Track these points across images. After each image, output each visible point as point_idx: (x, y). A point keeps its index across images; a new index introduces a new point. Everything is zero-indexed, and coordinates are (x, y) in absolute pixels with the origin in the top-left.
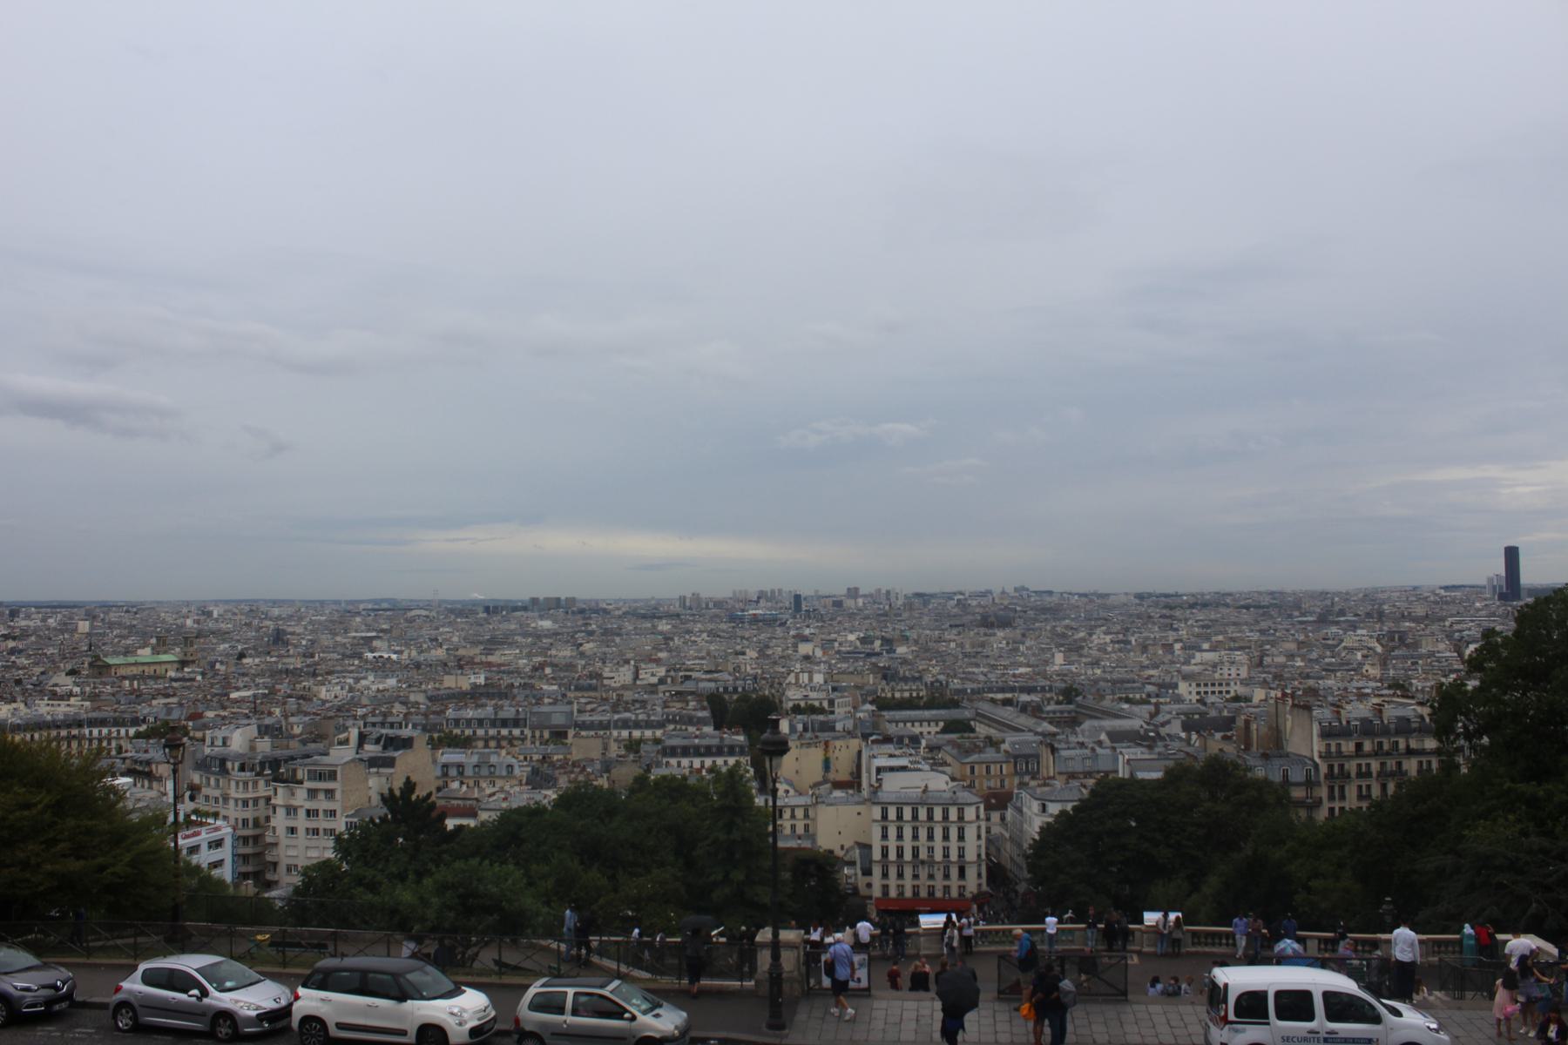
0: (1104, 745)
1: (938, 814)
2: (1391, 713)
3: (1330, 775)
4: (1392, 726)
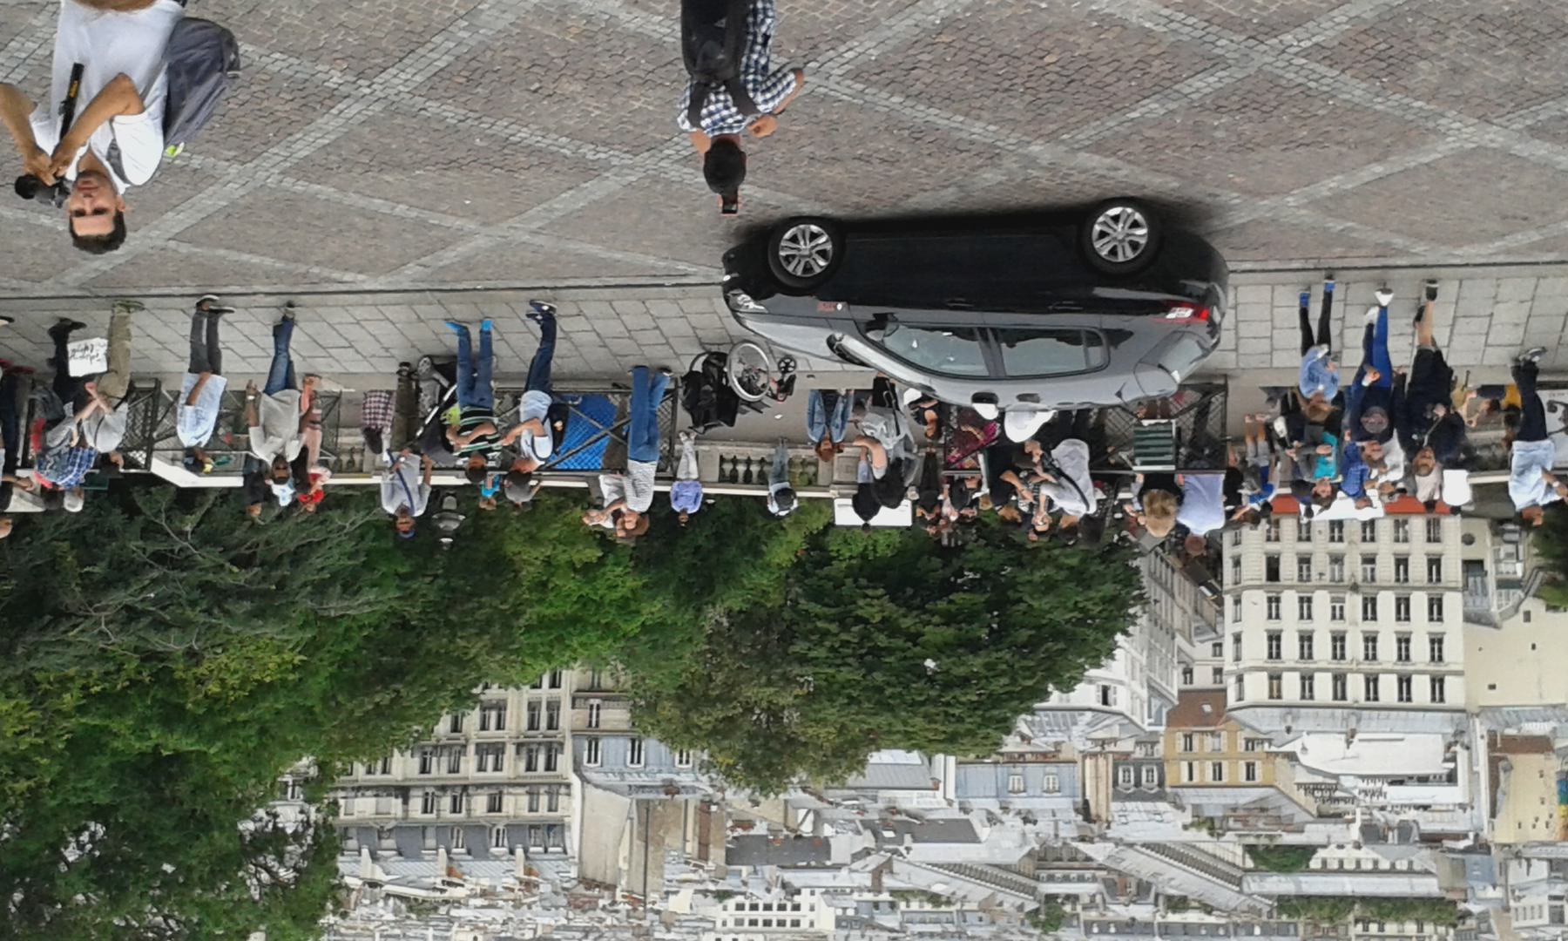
0: (984, 816)
1: (1323, 687)
2: (431, 869)
3: (553, 750)
4: (431, 842)
